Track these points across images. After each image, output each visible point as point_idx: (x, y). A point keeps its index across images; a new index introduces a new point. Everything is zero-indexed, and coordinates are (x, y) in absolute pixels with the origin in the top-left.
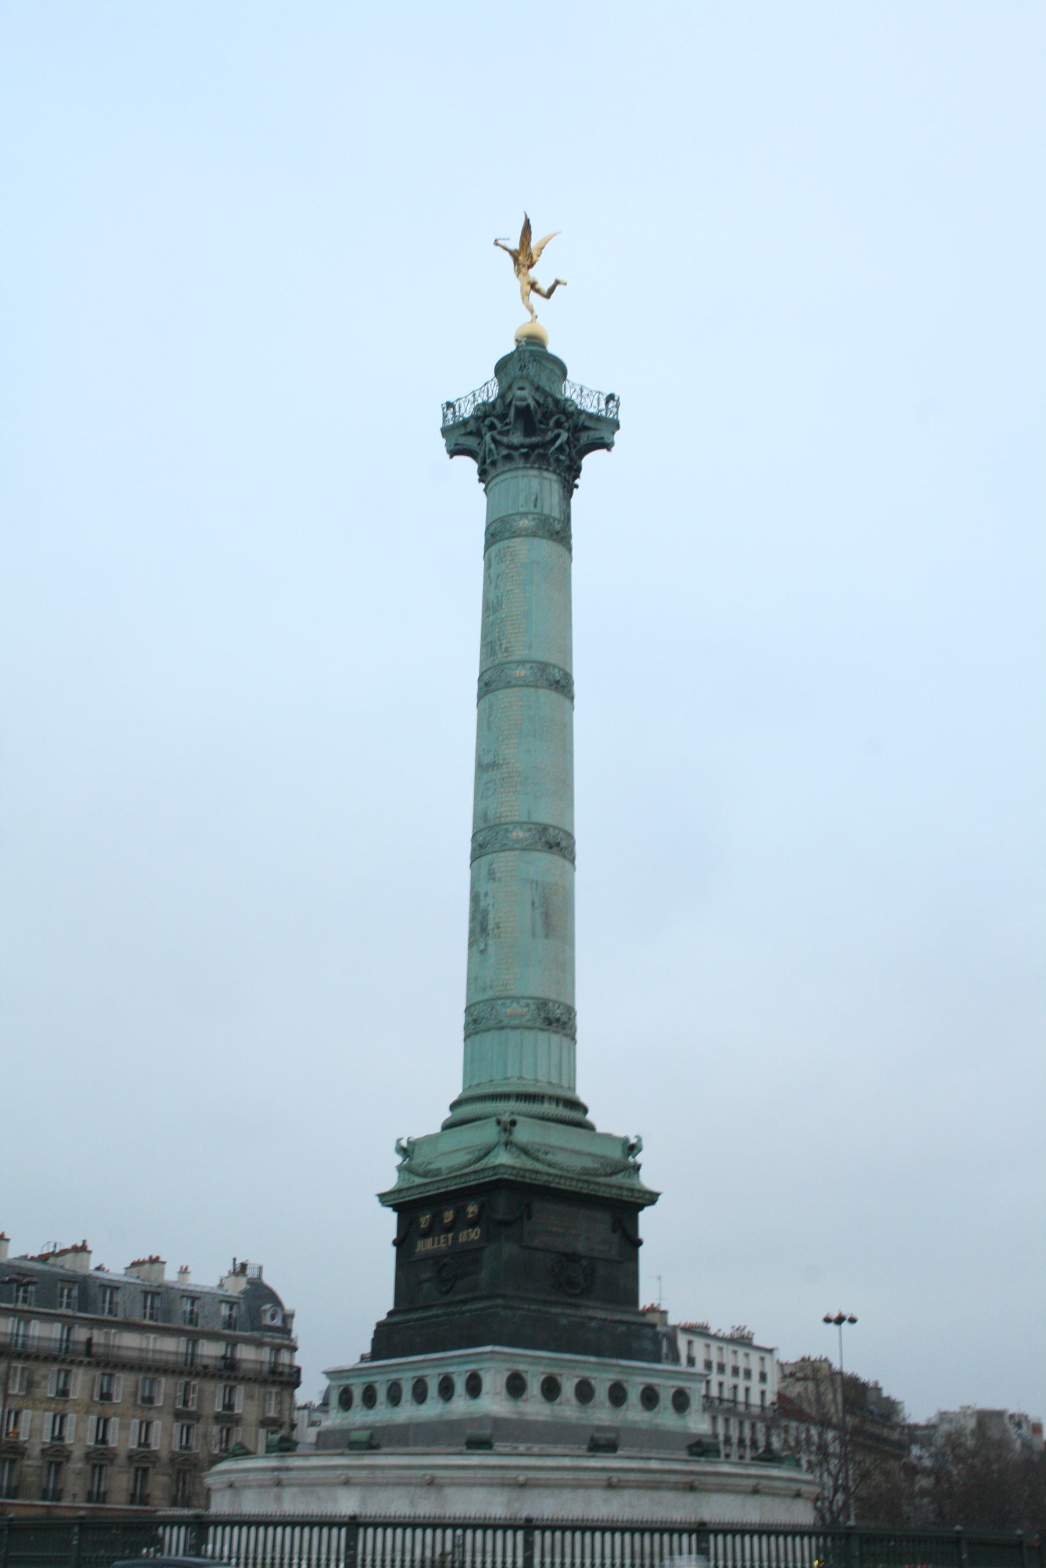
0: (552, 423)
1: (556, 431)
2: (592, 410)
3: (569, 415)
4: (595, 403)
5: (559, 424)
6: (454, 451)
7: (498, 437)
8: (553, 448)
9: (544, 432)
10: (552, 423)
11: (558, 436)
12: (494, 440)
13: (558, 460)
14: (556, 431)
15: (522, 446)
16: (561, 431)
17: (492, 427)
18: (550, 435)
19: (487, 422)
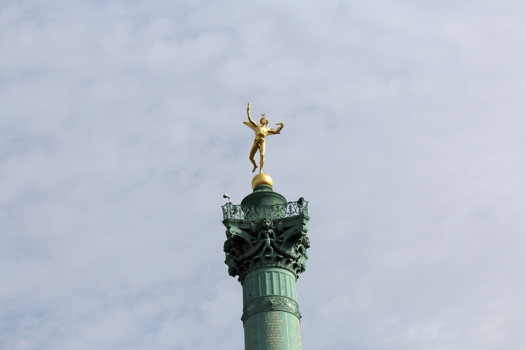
0: (259, 236)
1: (262, 241)
2: (287, 216)
3: (266, 228)
4: (288, 211)
5: (263, 236)
6: (232, 273)
7: (237, 259)
8: (263, 252)
9: (254, 245)
10: (259, 236)
11: (264, 243)
12: (235, 260)
13: (268, 258)
14: (262, 241)
15: (244, 260)
16: (265, 239)
17: (233, 253)
18: (259, 245)
19: (231, 250)
